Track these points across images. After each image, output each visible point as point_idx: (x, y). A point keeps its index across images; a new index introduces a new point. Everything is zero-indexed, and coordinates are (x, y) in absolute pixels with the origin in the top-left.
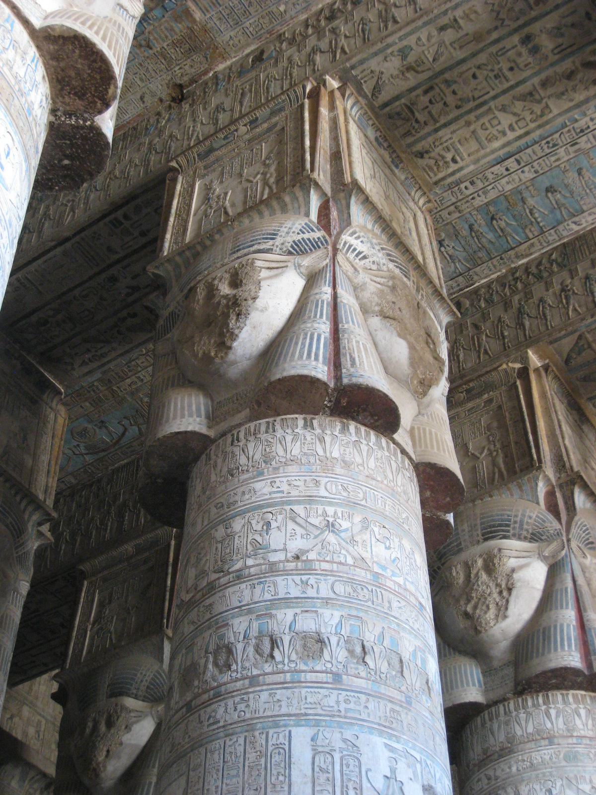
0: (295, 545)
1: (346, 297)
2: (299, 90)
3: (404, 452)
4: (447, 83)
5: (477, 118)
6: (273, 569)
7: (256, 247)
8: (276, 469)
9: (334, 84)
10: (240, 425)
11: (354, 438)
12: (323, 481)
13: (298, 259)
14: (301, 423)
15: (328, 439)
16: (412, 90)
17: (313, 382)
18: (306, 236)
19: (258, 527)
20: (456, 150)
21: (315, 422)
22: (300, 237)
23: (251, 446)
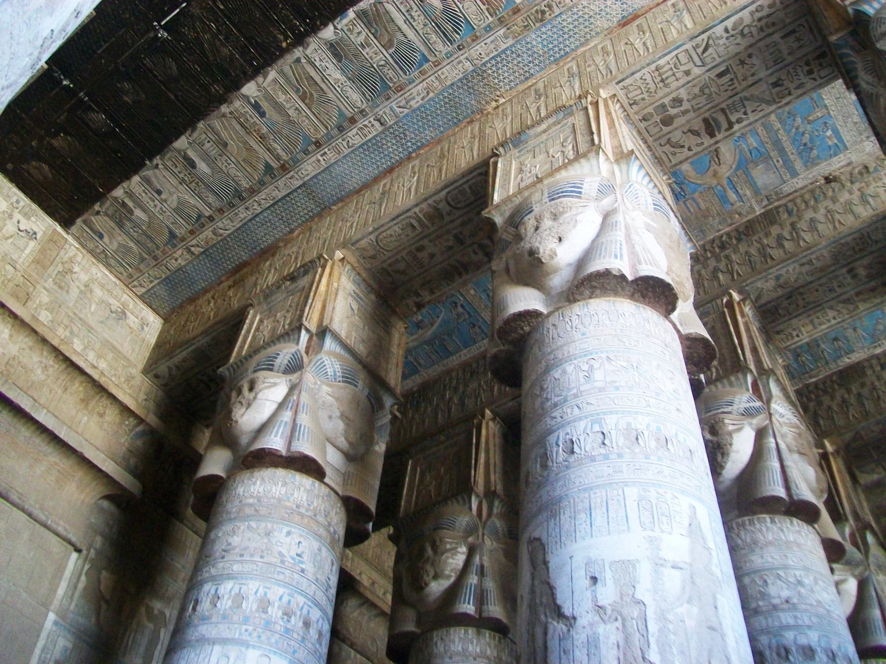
0: (785, 593)
1: (783, 446)
2: (719, 301)
3: (818, 533)
4: (801, 294)
5: (815, 313)
6: (775, 607)
7: (722, 410)
8: (761, 548)
9: (736, 297)
10: (731, 520)
11: (797, 528)
12: (790, 555)
13: (749, 420)
14: (768, 520)
15: (785, 530)
16: (778, 298)
17: (778, 499)
18: (752, 404)
19: (760, 582)
20: (800, 331)
21: (776, 520)
22: (747, 405)
23: (742, 533)
